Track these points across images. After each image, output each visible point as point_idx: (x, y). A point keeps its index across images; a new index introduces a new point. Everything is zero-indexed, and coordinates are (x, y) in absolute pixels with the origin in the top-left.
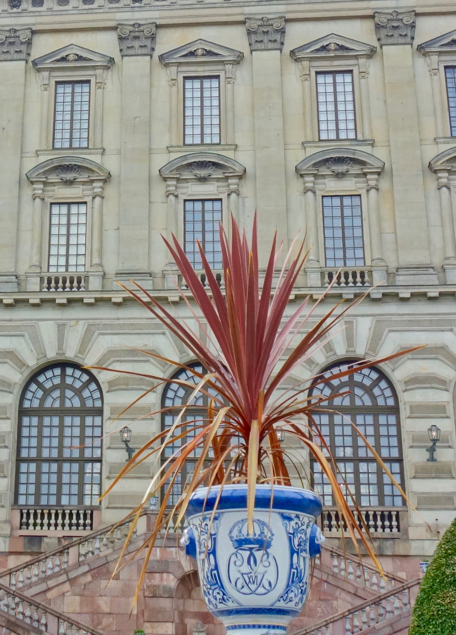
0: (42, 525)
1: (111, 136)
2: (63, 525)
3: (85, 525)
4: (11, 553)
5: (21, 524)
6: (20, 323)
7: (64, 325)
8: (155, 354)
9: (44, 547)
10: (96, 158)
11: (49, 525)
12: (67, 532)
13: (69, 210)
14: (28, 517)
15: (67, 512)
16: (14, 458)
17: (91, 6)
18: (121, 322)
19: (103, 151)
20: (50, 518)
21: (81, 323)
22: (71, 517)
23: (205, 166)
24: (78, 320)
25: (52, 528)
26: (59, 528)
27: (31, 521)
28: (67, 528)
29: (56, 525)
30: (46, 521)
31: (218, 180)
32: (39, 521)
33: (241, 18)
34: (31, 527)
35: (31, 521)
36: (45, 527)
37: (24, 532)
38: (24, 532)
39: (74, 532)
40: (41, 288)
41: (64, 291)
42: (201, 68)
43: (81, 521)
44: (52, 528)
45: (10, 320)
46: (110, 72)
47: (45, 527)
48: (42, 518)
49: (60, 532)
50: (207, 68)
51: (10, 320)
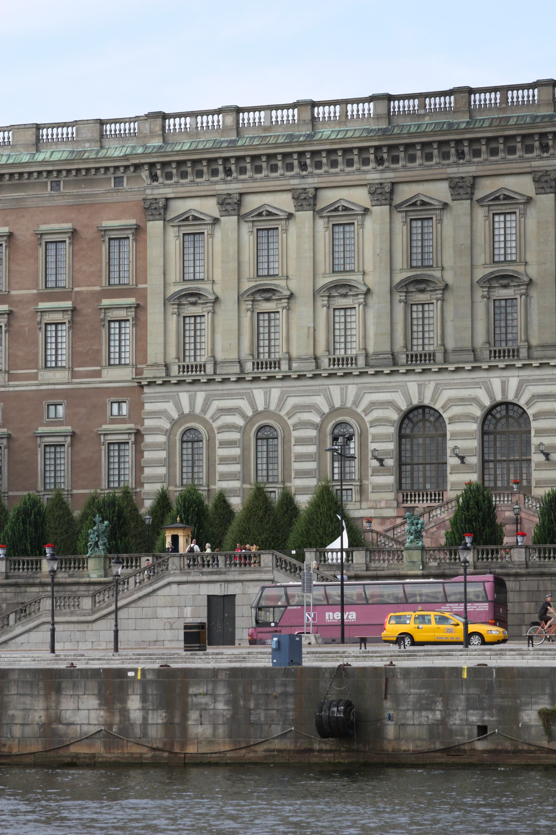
0: (415, 501)
2: (427, 500)
3: (439, 500)
4: (398, 517)
5: (403, 501)
6: (395, 384)
7: (421, 384)
8: (475, 400)
9: (416, 513)
10: (437, 274)
11: (419, 500)
12: (429, 504)
13: (423, 308)
14: (407, 497)
15: (429, 493)
16: (397, 464)
17: (431, 163)
18: (455, 381)
19: (443, 269)
20: (419, 496)
21: (432, 382)
22: (431, 496)
23: (506, 279)
24: (430, 381)
25: (421, 502)
26: (425, 502)
27: (409, 499)
28: (429, 502)
29: (423, 500)
30: (417, 498)
31: (514, 286)
32: (413, 498)
33: (529, 170)
34: (409, 502)
35: (409, 499)
36: (417, 502)
37: (405, 505)
38: (405, 505)
39: (433, 504)
40: (407, 361)
42: (504, 207)
43: (437, 498)
44: (421, 502)
45: (390, 382)
46: (445, 211)
47: (417, 502)
48: (415, 497)
49: (425, 505)
50: (508, 207)
51: (390, 382)
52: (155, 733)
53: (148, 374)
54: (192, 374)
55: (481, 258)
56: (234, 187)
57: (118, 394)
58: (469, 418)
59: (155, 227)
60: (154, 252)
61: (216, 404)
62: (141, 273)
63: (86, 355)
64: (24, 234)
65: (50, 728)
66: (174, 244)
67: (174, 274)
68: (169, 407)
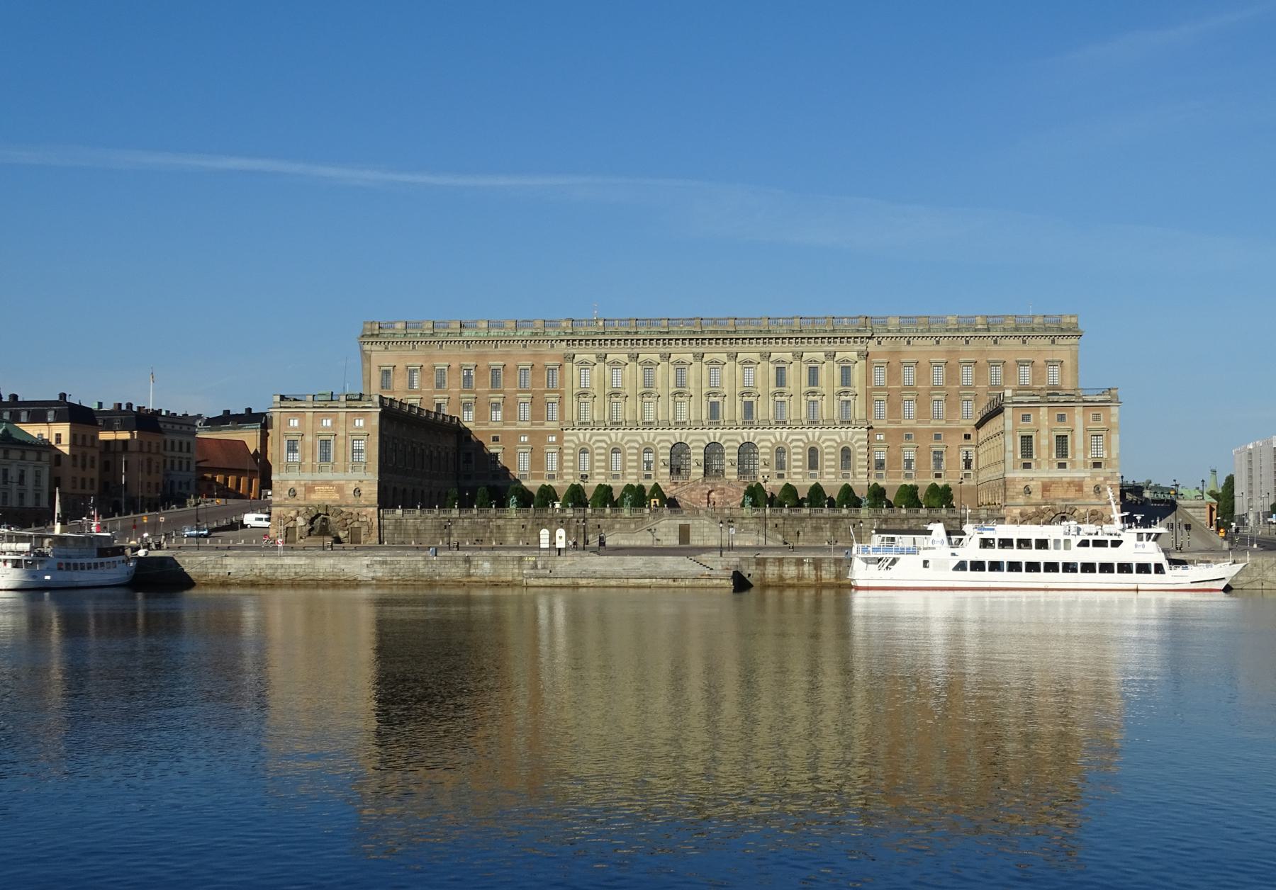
1: (692, 384)
41: (680, 425)
52: (813, 577)
53: (565, 425)
54: (584, 425)
55: (705, 384)
56: (603, 351)
57: (552, 433)
58: (700, 447)
59: (568, 365)
60: (568, 375)
61: (594, 438)
62: (562, 384)
63: (538, 416)
64: (510, 365)
65: (781, 578)
66: (576, 372)
67: (576, 385)
68: (574, 438)
